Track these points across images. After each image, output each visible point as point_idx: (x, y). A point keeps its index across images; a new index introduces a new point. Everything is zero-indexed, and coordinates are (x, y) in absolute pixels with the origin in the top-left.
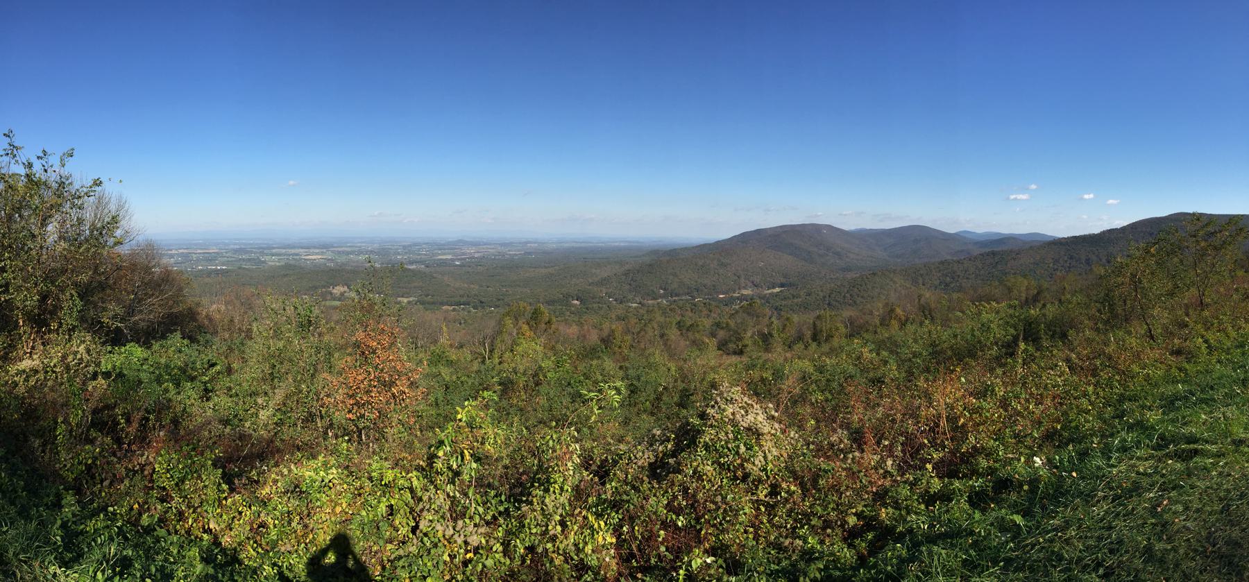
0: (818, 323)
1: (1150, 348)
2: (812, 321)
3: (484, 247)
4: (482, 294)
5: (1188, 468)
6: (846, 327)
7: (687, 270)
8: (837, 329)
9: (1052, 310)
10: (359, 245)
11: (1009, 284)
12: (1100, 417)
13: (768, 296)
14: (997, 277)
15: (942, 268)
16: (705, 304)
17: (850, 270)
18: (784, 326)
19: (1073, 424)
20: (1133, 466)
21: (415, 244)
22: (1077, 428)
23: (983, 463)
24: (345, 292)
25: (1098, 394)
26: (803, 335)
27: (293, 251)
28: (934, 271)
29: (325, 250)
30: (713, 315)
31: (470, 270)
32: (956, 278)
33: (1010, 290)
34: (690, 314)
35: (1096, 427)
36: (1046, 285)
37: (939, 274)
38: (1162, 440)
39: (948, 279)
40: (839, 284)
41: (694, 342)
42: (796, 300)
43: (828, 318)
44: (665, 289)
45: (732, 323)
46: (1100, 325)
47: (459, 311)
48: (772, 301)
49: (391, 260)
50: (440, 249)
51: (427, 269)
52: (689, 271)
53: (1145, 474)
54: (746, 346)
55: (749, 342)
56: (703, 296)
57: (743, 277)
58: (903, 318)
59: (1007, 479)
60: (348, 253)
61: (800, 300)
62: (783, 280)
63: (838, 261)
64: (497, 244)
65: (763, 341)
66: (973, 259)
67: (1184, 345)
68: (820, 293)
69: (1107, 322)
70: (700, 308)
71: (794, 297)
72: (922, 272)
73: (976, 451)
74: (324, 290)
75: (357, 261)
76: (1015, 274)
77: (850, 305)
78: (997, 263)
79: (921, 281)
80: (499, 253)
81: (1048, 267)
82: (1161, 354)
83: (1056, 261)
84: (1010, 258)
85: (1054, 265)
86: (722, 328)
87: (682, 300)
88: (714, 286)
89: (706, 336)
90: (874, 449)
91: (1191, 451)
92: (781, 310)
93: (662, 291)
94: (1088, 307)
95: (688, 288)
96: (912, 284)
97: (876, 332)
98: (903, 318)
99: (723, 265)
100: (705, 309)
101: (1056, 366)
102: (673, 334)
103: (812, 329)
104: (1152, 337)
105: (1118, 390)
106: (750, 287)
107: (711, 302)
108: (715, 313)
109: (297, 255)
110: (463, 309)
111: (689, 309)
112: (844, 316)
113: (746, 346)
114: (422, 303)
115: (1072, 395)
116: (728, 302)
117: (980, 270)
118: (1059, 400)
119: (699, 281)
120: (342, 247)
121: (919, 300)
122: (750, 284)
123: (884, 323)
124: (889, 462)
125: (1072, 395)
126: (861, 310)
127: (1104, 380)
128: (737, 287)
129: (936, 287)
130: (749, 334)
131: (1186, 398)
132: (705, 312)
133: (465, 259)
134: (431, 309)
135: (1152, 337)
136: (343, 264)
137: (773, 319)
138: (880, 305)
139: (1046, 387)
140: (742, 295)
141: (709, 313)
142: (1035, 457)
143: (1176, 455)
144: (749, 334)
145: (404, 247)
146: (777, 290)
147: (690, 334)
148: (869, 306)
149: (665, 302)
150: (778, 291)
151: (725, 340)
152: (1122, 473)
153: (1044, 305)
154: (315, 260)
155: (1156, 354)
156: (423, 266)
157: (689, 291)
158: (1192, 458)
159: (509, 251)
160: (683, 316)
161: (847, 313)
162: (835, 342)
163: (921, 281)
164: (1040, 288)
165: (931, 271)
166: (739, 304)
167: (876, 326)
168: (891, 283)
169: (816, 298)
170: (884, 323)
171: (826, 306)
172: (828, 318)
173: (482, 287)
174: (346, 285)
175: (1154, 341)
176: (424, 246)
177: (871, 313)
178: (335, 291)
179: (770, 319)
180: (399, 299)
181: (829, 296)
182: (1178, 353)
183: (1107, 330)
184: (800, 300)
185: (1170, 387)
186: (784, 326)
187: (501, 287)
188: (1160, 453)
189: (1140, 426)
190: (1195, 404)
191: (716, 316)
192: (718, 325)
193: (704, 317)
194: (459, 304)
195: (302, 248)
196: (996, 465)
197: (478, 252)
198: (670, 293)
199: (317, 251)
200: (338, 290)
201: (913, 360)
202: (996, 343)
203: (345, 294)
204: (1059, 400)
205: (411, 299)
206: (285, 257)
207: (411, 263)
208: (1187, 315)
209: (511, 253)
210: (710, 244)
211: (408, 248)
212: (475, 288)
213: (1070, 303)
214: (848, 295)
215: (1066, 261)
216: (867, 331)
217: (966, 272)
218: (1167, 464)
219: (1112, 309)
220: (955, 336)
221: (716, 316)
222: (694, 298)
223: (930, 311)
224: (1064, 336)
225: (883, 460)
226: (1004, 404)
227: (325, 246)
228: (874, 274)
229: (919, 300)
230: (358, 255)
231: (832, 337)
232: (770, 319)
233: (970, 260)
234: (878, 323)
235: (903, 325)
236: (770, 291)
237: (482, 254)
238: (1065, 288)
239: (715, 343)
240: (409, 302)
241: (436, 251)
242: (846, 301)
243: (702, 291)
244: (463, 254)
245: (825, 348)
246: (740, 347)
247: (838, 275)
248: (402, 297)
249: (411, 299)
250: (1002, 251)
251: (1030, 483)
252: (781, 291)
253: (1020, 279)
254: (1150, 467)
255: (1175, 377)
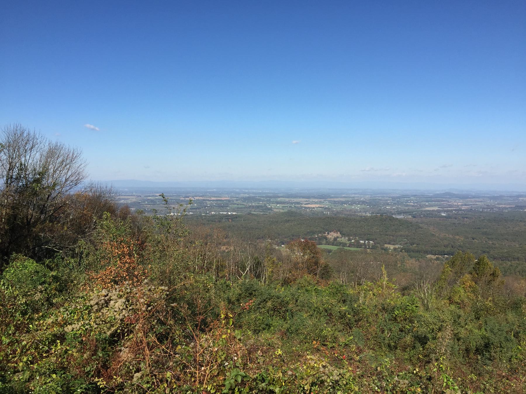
3: (473, 200)
4: (467, 245)
10: (353, 195)
21: (404, 196)
24: (338, 237)
27: (295, 200)
29: (323, 200)
31: (456, 221)
47: (443, 260)
49: (380, 210)
50: (427, 201)
51: (414, 219)
60: (343, 203)
64: (484, 197)
74: (320, 235)
75: (350, 210)
80: (488, 206)
109: (298, 203)
110: (447, 259)
114: (408, 251)
120: (337, 197)
133: (452, 211)
134: (415, 257)
136: (338, 212)
145: (393, 198)
154: (314, 208)
156: (410, 217)
159: (498, 204)
173: (468, 238)
174: (339, 231)
176: (412, 198)
178: (329, 236)
180: (386, 245)
187: (487, 240)
194: (443, 253)
195: (303, 197)
197: (466, 205)
199: (316, 200)
200: (332, 236)
203: (338, 239)
205: (397, 246)
206: (289, 205)
207: (399, 213)
209: (500, 206)
211: (398, 199)
212: (460, 239)
227: (323, 196)
230: (351, 204)
237: (470, 206)
240: (395, 249)
241: (424, 203)
244: (450, 206)
248: (389, 244)
249: (397, 246)
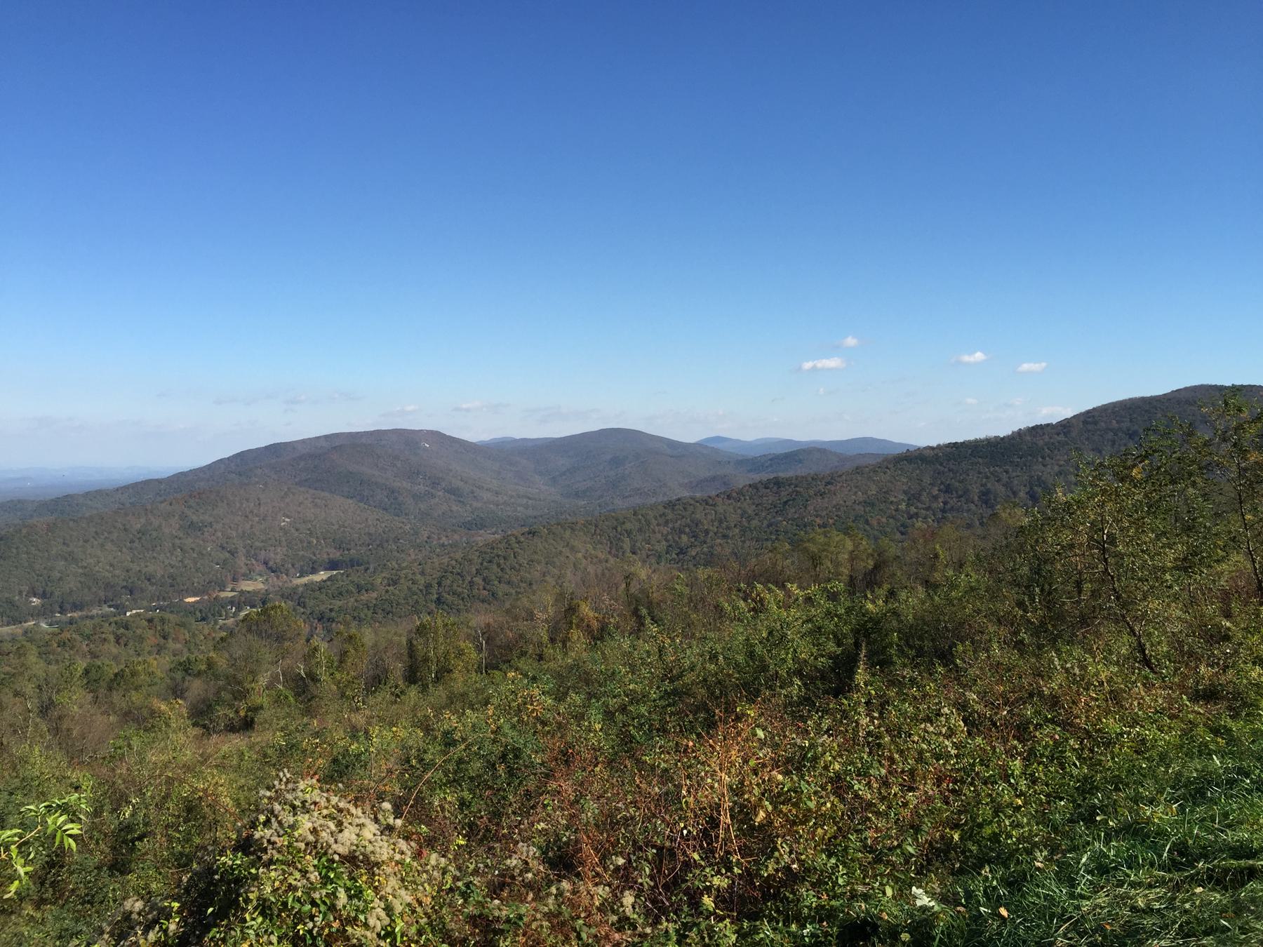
0: (419, 643)
1: (1144, 685)
2: (404, 640)
5: (1236, 902)
6: (479, 649)
7: (102, 545)
8: (460, 653)
9: (913, 602)
11: (813, 548)
12: (1042, 818)
13: (301, 589)
14: (786, 533)
15: (670, 517)
16: (150, 621)
17: (483, 526)
18: (343, 655)
19: (987, 831)
20: (1126, 896)
22: (995, 837)
23: (809, 898)
25: (1032, 775)
26: (386, 671)
28: (654, 522)
30: (171, 645)
32: (702, 536)
33: (815, 560)
34: (115, 650)
35: (1036, 835)
36: (893, 550)
37: (665, 530)
38: (1181, 854)
39: (685, 538)
40: (459, 555)
41: (127, 716)
42: (364, 597)
43: (441, 631)
44: (43, 595)
45: (222, 662)
46: (1024, 636)
48: (310, 603)
52: (109, 546)
53: (1149, 911)
54: (257, 709)
55: (263, 700)
56: (145, 603)
57: (242, 552)
58: (595, 625)
59: (864, 920)
61: (375, 595)
62: (336, 555)
63: (454, 508)
65: (297, 695)
66: (734, 494)
67: (1223, 680)
68: (418, 577)
69: (1038, 631)
70: (139, 632)
71: (359, 588)
72: (628, 526)
73: (792, 878)
76: (824, 526)
77: (483, 601)
78: (786, 503)
79: (627, 544)
81: (897, 510)
82: (1169, 699)
83: (913, 498)
84: (811, 492)
85: (908, 505)
86: (199, 674)
87: (92, 618)
88: (172, 577)
89: (158, 696)
90: (598, 874)
91: (1243, 872)
92: (331, 620)
93: (35, 601)
94: (994, 595)
95: (108, 586)
96: (610, 553)
97: (541, 657)
98: (595, 625)
99: (192, 528)
100: (151, 632)
101: (939, 714)
102: (75, 701)
103: (406, 658)
104: (1146, 662)
105: (1079, 770)
106: (261, 575)
107: (167, 616)
108: (176, 640)
111: (112, 638)
112: (473, 623)
113: (257, 709)
115: (977, 774)
116: (205, 614)
117: (749, 519)
118: (952, 782)
119: (135, 567)
121: (628, 585)
122: (261, 568)
123: (558, 636)
124: (628, 899)
125: (977, 774)
126: (508, 611)
127: (1045, 747)
128: (229, 578)
129: (660, 556)
130: (263, 680)
131: (1231, 783)
132: (151, 639)
135: (1146, 662)
137: (316, 641)
138: (549, 599)
139: (920, 758)
140: (242, 592)
141: (163, 641)
142: (914, 888)
143: (1210, 878)
144: (263, 680)
146: (322, 575)
147: (116, 697)
148: (525, 600)
149: (44, 625)
150: (325, 578)
151: (204, 701)
152: (1102, 908)
153: (892, 594)
155: (1159, 697)
157: (110, 595)
158: (1243, 885)
160: (94, 655)
161: (479, 619)
162: (459, 681)
163: (627, 544)
164: (879, 555)
165: (648, 524)
166: (235, 615)
167: (540, 644)
168: (566, 551)
169: (409, 589)
170: (558, 636)
171: (433, 606)
172: (441, 631)
175: (1151, 668)
177: (531, 616)
179: (308, 641)
181: (439, 584)
182: (1209, 695)
183: (1040, 647)
184: (375, 595)
185: (1197, 764)
186: (343, 655)
188: (1176, 876)
189: (1135, 831)
190: (1249, 792)
191: (178, 646)
192: (186, 668)
193: (149, 653)
196: (833, 903)
198: (55, 604)
201: (631, 708)
202: (799, 673)
204: (952, 782)
208: (1228, 616)
210: (159, 481)
213: (953, 586)
214: (478, 580)
215: (935, 498)
216: (523, 654)
217: (721, 522)
218: (1194, 894)
219: (1049, 600)
220: (714, 657)
221: (178, 646)
222: (121, 609)
223: (650, 605)
224: (946, 657)
225: (617, 897)
226: (839, 785)
228: (533, 533)
229: (628, 585)
231: (450, 671)
232: (308, 641)
233: (729, 497)
234: (545, 638)
235: (599, 635)
236: (305, 580)
238: (936, 556)
239: (184, 711)
242: (475, 592)
243: (142, 590)
245: (439, 693)
246: (242, 714)
247: (456, 537)
250: (797, 477)
251: (912, 929)
252: (329, 579)
253: (837, 537)
254: (1158, 899)
255: (1206, 745)
